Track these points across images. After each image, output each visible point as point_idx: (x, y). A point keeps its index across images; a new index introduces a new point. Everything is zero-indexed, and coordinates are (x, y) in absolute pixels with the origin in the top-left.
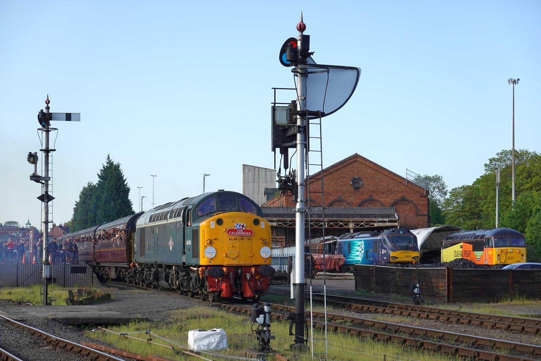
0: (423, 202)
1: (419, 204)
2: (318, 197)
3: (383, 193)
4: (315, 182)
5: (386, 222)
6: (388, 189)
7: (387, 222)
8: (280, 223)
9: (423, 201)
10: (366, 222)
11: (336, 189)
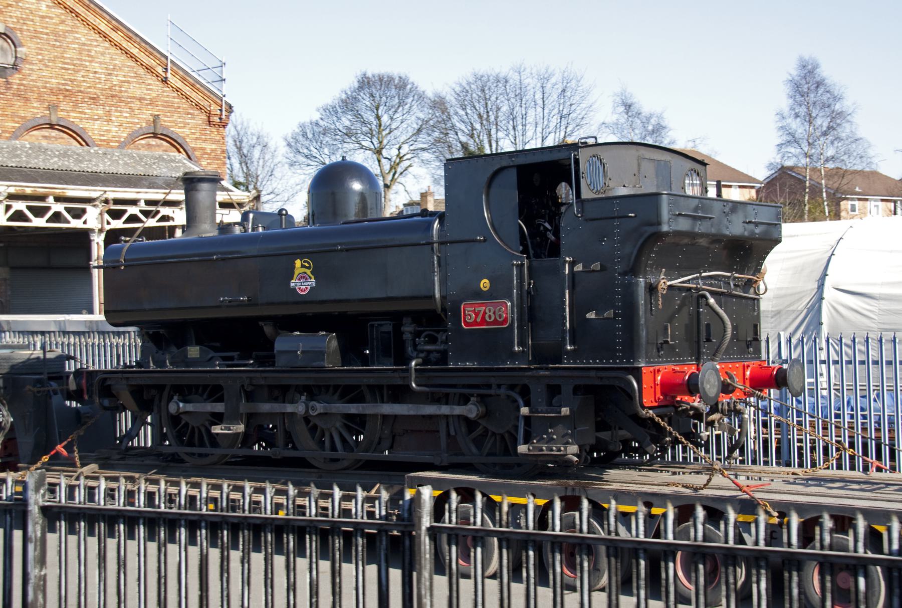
0: (214, 147)
3: (95, 99)
6: (111, 89)
10: (149, 203)
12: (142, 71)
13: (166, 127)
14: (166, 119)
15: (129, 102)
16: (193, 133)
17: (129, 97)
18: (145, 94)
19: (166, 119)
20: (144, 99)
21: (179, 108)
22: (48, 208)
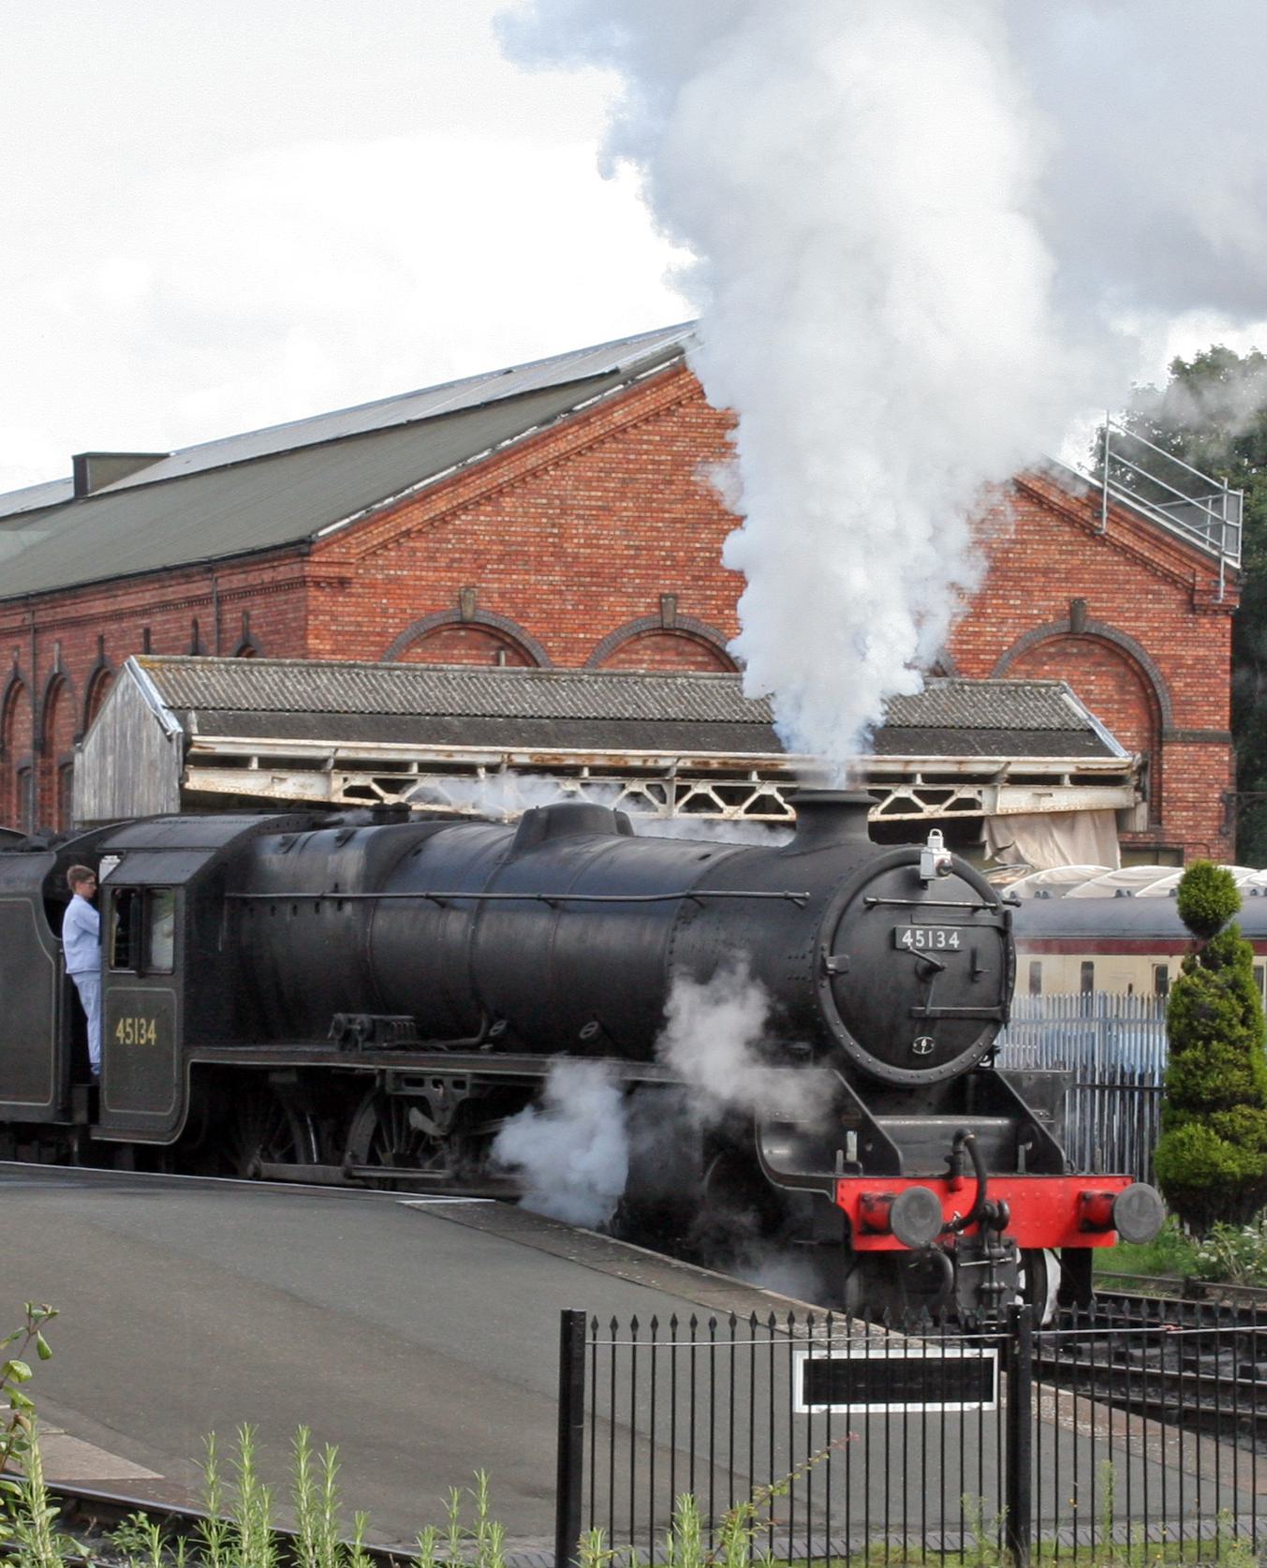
0: (1201, 652)
1: (1178, 662)
2: (527, 602)
4: (511, 494)
5: (1053, 780)
7: (1067, 780)
8: (359, 780)
9: (1199, 643)
10: (928, 778)
11: (648, 549)
12: (1050, 521)
13: (1100, 620)
14: (1098, 605)
15: (1022, 579)
16: (1158, 629)
17: (1021, 570)
18: (1056, 562)
19: (1098, 605)
20: (1055, 571)
21: (1128, 582)
22: (752, 790)
